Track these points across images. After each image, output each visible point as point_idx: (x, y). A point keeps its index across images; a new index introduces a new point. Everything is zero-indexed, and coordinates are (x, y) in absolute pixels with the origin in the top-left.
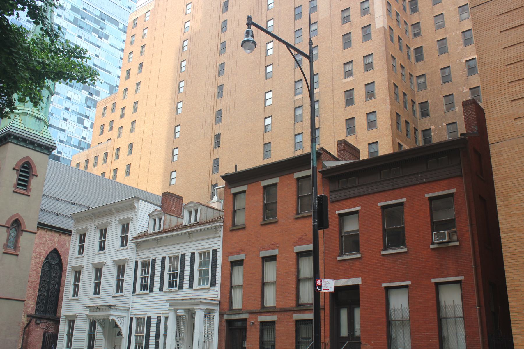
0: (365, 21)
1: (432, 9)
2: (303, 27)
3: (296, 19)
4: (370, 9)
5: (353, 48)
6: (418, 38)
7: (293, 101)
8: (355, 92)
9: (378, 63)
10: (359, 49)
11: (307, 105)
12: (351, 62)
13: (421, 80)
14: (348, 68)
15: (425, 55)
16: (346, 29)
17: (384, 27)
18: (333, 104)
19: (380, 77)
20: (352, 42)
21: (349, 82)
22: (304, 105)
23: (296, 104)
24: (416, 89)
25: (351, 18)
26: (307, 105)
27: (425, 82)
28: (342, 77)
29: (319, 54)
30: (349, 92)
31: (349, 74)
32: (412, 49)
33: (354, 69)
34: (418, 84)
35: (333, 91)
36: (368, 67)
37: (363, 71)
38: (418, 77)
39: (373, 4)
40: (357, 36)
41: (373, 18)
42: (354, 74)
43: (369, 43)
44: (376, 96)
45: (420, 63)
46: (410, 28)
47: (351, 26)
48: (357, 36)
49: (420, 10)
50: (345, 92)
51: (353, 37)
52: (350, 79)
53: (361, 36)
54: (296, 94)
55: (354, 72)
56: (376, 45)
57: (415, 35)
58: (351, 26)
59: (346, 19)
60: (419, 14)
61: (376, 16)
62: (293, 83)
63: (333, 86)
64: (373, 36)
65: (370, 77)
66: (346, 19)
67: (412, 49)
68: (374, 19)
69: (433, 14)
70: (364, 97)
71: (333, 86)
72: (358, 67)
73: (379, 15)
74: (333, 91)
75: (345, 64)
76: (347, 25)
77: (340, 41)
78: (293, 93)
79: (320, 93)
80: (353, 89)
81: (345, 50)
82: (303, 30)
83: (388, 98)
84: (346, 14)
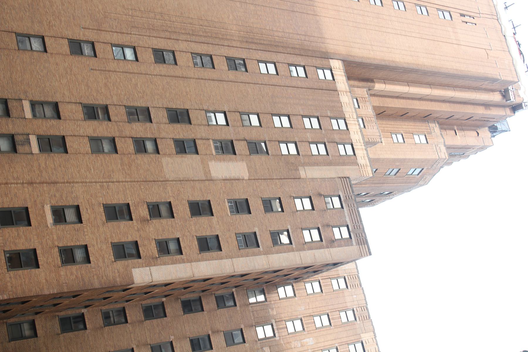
0: (149, 248)
1: (145, 344)
2: (154, 125)
3: (169, 110)
4: (166, 258)
5: (104, 224)
6: (100, 320)
7: (22, 96)
8: (22, 229)
9: (72, 274)
10: (98, 235)
11: (11, 127)
12: (80, 221)
13: (27, 332)
14: (70, 215)
15: (70, 334)
16: (140, 211)
17: (133, 283)
18: (7, 183)
19: (48, 278)
20: (115, 223)
21: (44, 216)
22: (10, 119)
23: (15, 104)
24: (12, 320)
25: (156, 222)
26: (11, 127)
27: (22, 337)
28: (54, 202)
29: (101, 156)
30: (25, 218)
31: (59, 215)
32: (84, 311)
33: (68, 227)
34: (20, 324)
35: (31, 183)
36: (68, 255)
37: (61, 245)
38: (33, 325)
39: (173, 263)
40: (124, 231)
41: (152, 262)
42: (58, 226)
43: (109, 255)
44: (12, 273)
45: (57, 328)
46: (119, 306)
47: (144, 221)
48: (124, 231)
49: (148, 322)
50: (27, 209)
51: (123, 225)
52: (50, 218)
53: (123, 240)
54: (33, 104)
55: (62, 227)
56: (104, 270)
57: (106, 316)
58: (144, 221)
59: (155, 210)
60: (141, 322)
61: (153, 269)
62: (55, 100)
63: (40, 183)
64: (120, 264)
65: (48, 258)
66: (155, 210)
67: (84, 311)
68: (149, 265)
69: (138, 346)
70: (14, 248)
71: (40, 183)
72: (68, 235)
73: (154, 275)
74: (31, 183)
75: (77, 208)
76: (144, 212)
77: (118, 199)
78: (37, 98)
79: (29, 156)
80: (29, 224)
81: (102, 209)
82: (148, 124)
83: (6, 297)
84: (164, 210)
